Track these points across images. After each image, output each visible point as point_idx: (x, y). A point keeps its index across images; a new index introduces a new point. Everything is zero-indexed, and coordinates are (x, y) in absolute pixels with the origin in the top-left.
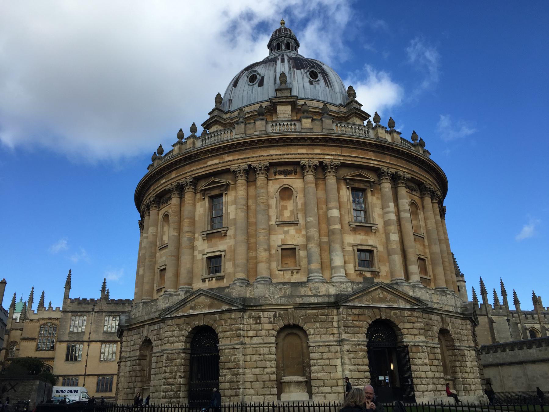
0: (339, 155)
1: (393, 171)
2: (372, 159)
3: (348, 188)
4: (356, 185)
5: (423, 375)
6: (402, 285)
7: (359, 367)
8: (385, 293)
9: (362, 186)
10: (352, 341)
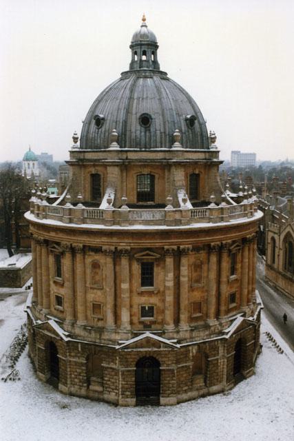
2: (157, 243)
5: (171, 385)
9: (150, 261)
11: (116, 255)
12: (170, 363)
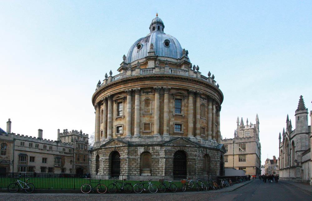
0: (110, 92)
1: (130, 90)
2: (122, 88)
3: (115, 104)
4: (119, 101)
5: (125, 168)
7: (106, 166)
9: (121, 101)
11: (106, 100)
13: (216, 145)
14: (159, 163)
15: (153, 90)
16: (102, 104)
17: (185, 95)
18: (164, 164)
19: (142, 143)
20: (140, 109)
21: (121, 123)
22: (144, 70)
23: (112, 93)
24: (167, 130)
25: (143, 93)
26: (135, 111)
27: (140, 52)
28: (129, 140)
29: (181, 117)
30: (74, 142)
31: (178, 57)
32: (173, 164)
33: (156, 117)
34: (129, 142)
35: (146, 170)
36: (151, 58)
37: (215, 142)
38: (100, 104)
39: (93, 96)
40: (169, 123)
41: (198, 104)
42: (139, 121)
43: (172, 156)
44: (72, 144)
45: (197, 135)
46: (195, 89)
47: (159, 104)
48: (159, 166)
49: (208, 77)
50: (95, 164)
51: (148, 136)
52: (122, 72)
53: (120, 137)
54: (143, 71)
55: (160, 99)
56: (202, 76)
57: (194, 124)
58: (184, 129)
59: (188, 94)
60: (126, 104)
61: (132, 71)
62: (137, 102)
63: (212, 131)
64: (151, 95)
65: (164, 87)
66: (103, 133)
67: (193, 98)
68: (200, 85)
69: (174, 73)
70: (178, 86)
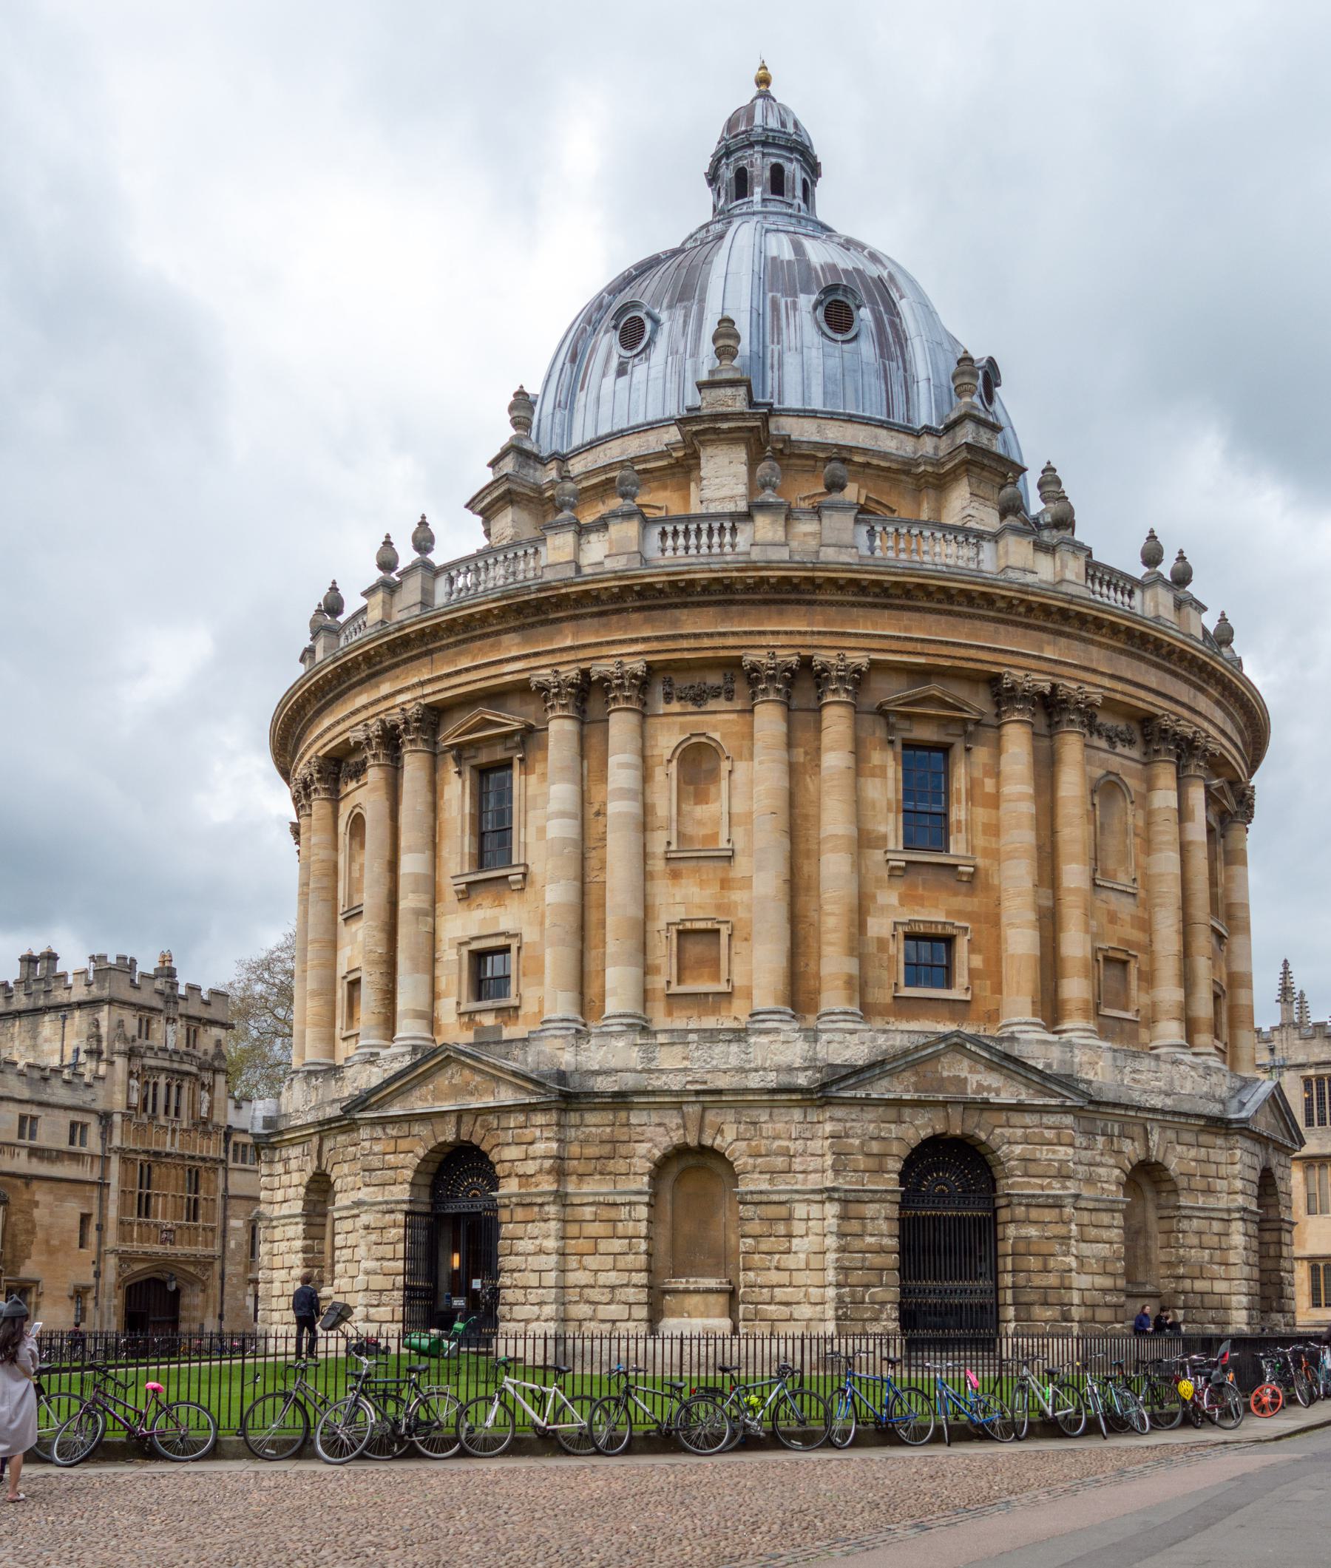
3: (459, 773)
4: (484, 757)
5: (533, 1279)
6: (540, 1039)
8: (467, 1072)
9: (499, 754)
10: (380, 1203)
11: (391, 740)
12: (531, 1167)
13: (1222, 1085)
14: (790, 1236)
15: (737, 678)
16: (359, 771)
17: (975, 716)
18: (831, 1242)
19: (664, 1078)
20: (645, 824)
21: (502, 928)
22: (669, 528)
23: (432, 693)
24: (849, 982)
25: (668, 703)
26: (609, 837)
27: (639, 371)
28: (567, 1059)
29: (945, 877)
30: (111, 1063)
31: (925, 415)
32: (893, 1243)
33: (762, 883)
34: (561, 1076)
35: (697, 1291)
36: (725, 426)
37: (1214, 1062)
38: (339, 767)
39: (282, 705)
40: (862, 926)
41: (1071, 784)
42: (641, 914)
43: (890, 1182)
44: (97, 1078)
45: (1070, 1016)
46: (1045, 666)
47: (787, 785)
48: (789, 1261)
49: (1146, 570)
50: (299, 1244)
51: (710, 1022)
52: (507, 522)
53: (497, 1029)
54: (663, 534)
55: (790, 744)
56: (1095, 571)
57: (1041, 929)
58: (972, 973)
59: (998, 705)
60: (544, 776)
61: (582, 531)
62: (620, 769)
63: (1187, 980)
64: (719, 717)
65: (821, 657)
66: (369, 998)
67: (1035, 735)
68: (1084, 640)
69: (891, 554)
70: (919, 647)
